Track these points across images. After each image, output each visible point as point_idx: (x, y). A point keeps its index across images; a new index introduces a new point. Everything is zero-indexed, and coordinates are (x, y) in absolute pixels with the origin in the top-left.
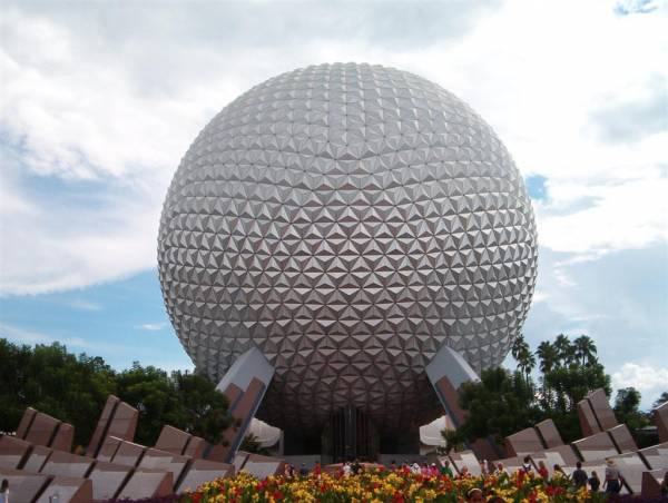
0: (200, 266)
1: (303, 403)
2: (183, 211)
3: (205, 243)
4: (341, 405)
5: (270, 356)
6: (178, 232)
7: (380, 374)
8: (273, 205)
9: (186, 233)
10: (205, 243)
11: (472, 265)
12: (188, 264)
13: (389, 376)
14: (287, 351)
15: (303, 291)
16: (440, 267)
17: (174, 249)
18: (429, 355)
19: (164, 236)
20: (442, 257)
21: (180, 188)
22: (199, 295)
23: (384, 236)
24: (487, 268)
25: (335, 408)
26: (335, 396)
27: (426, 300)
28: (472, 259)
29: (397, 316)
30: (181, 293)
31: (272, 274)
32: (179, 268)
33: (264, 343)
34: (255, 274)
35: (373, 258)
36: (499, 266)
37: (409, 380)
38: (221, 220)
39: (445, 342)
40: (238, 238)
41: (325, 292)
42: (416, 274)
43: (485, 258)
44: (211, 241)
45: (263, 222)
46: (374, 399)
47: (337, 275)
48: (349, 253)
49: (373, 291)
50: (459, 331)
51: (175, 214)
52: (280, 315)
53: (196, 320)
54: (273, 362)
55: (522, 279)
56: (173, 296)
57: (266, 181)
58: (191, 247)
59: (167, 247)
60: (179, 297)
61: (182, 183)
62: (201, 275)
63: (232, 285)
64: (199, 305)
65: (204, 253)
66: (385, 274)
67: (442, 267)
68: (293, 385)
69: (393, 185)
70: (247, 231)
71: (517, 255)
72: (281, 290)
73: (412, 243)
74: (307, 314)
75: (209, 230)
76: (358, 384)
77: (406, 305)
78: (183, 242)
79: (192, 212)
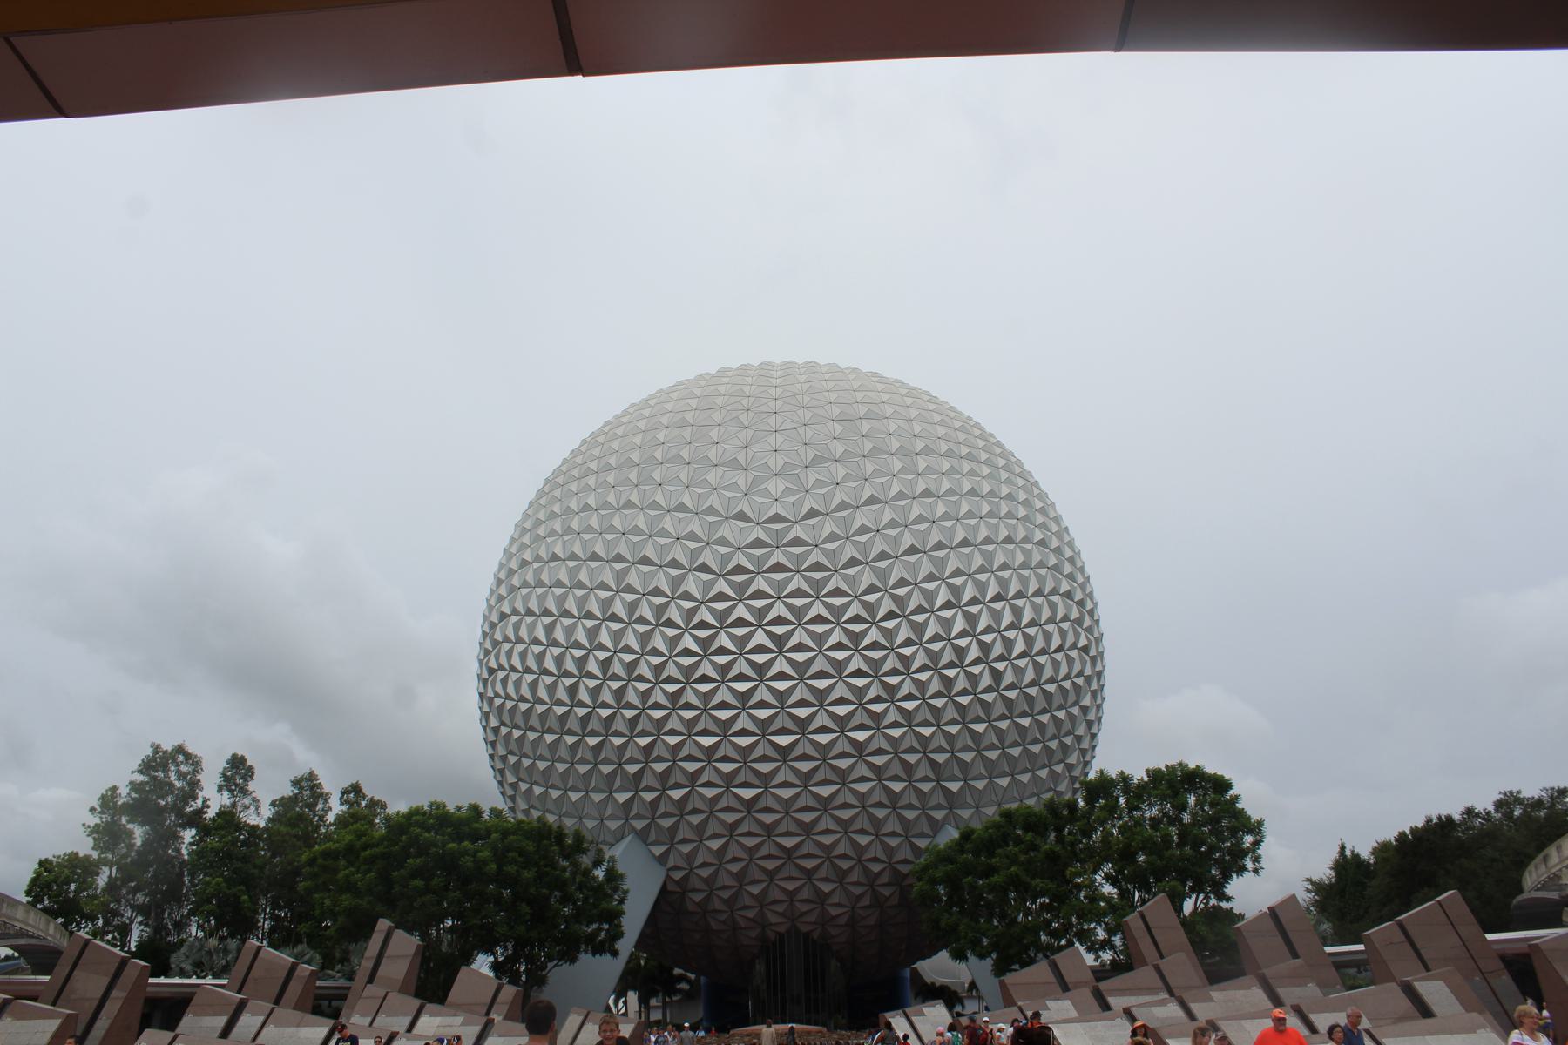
0: (543, 702)
1: (714, 925)
2: (515, 612)
3: (549, 664)
4: (782, 929)
5: (658, 850)
6: (507, 646)
7: (842, 875)
8: (658, 601)
9: (520, 647)
10: (549, 664)
11: (988, 690)
12: (523, 699)
13: (855, 879)
14: (685, 841)
15: (706, 741)
16: (934, 696)
17: (501, 674)
19: (487, 653)
20: (936, 680)
21: (511, 572)
22: (542, 750)
23: (839, 646)
24: (1012, 694)
25: (772, 936)
26: (769, 914)
27: (911, 750)
28: (986, 681)
29: (863, 779)
30: (513, 746)
31: (658, 714)
32: (509, 704)
33: (648, 827)
34: (629, 714)
35: (822, 684)
36: (1033, 691)
38: (574, 626)
39: (945, 820)
40: (602, 655)
41: (744, 741)
42: (892, 708)
43: (1009, 678)
44: (559, 660)
45: (642, 629)
46: (833, 918)
47: (763, 714)
48: (782, 676)
49: (824, 739)
50: (969, 800)
51: (503, 616)
52: (671, 782)
53: (538, 790)
54: (662, 859)
55: (1075, 711)
56: (501, 751)
57: (646, 561)
58: (528, 670)
59: (491, 671)
60: (511, 753)
61: (514, 565)
62: (543, 717)
63: (593, 733)
64: (542, 765)
65: (548, 680)
66: (842, 710)
67: (938, 695)
68: (698, 897)
69: (853, 562)
70: (616, 644)
71: (1064, 670)
72: (673, 740)
73: (886, 657)
75: (555, 644)
76: (805, 894)
77: (879, 760)
78: (516, 662)
79: (529, 612)
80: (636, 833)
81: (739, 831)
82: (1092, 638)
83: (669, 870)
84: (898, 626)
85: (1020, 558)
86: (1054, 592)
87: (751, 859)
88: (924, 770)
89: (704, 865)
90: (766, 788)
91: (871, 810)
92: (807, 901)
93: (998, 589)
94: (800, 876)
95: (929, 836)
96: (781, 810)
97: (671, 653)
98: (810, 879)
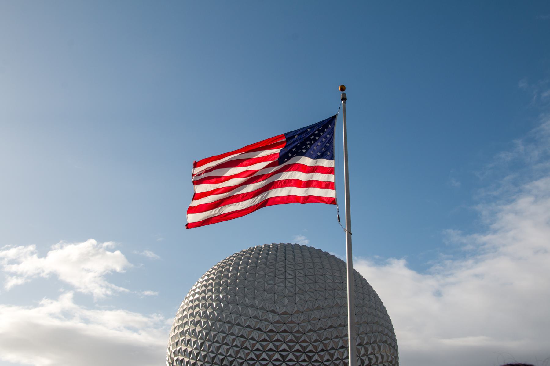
82: (393, 357)
84: (325, 354)
85: (368, 329)
86: (381, 341)
93: (360, 341)
97: (246, 358)
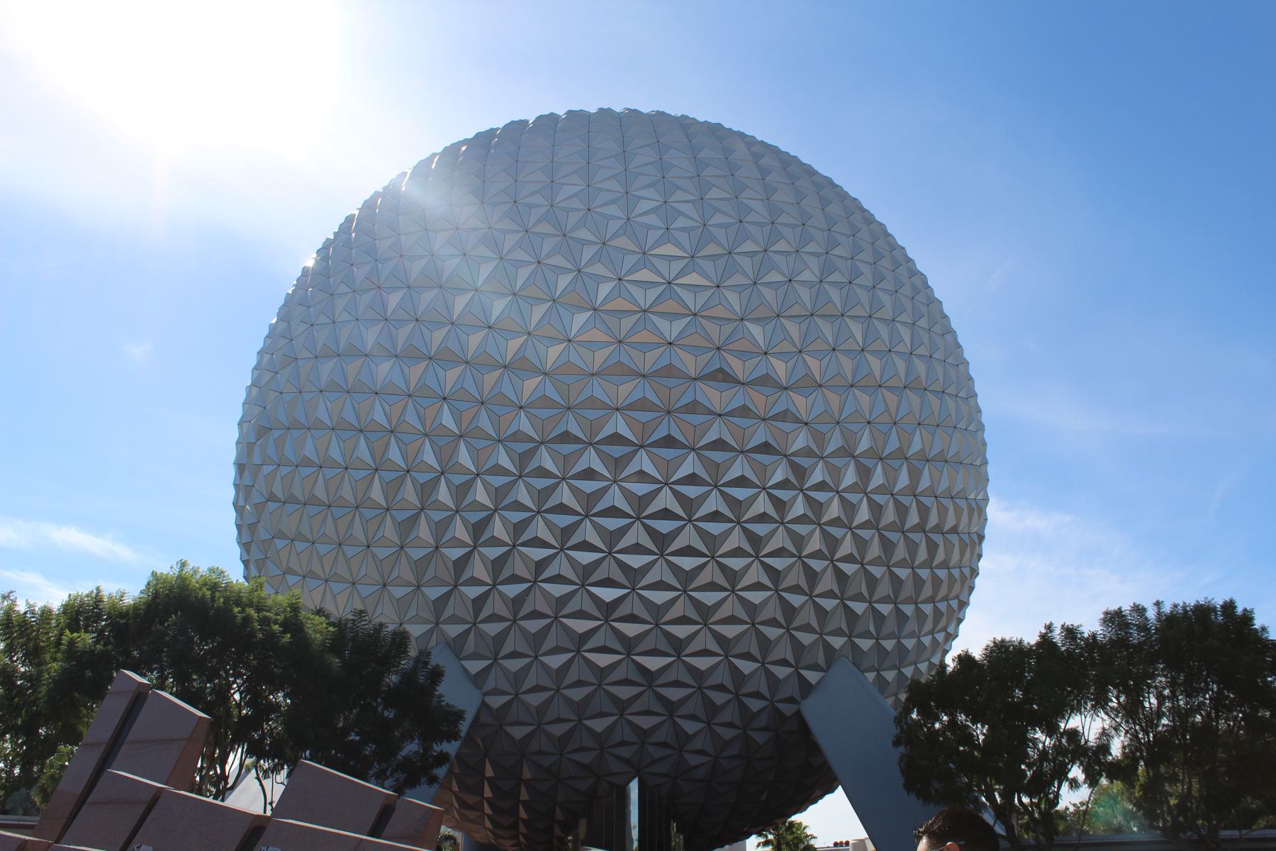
5: (475, 666)
14: (515, 655)
18: (812, 676)
37: (765, 729)
68: (518, 732)
74: (568, 572)
76: (661, 736)
80: (448, 644)
81: (589, 645)
83: (485, 694)
87: (600, 685)
88: (827, 582)
89: (538, 689)
90: (633, 589)
91: (762, 628)
92: (664, 745)
94: (660, 712)
95: (824, 671)
96: (651, 621)
98: (671, 716)
